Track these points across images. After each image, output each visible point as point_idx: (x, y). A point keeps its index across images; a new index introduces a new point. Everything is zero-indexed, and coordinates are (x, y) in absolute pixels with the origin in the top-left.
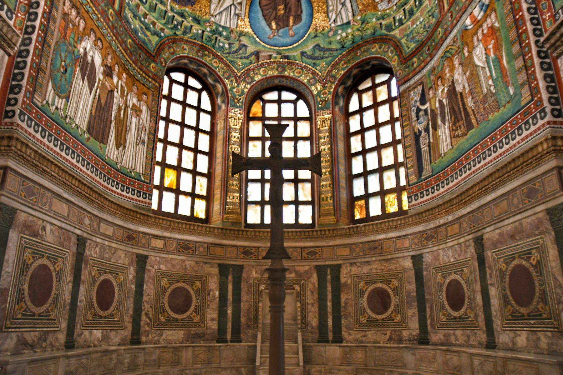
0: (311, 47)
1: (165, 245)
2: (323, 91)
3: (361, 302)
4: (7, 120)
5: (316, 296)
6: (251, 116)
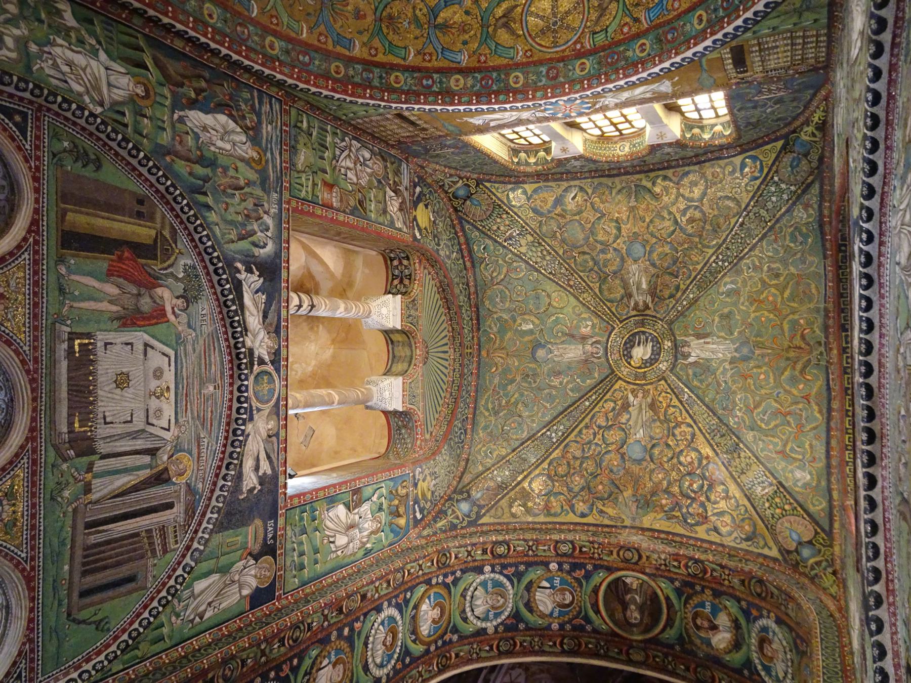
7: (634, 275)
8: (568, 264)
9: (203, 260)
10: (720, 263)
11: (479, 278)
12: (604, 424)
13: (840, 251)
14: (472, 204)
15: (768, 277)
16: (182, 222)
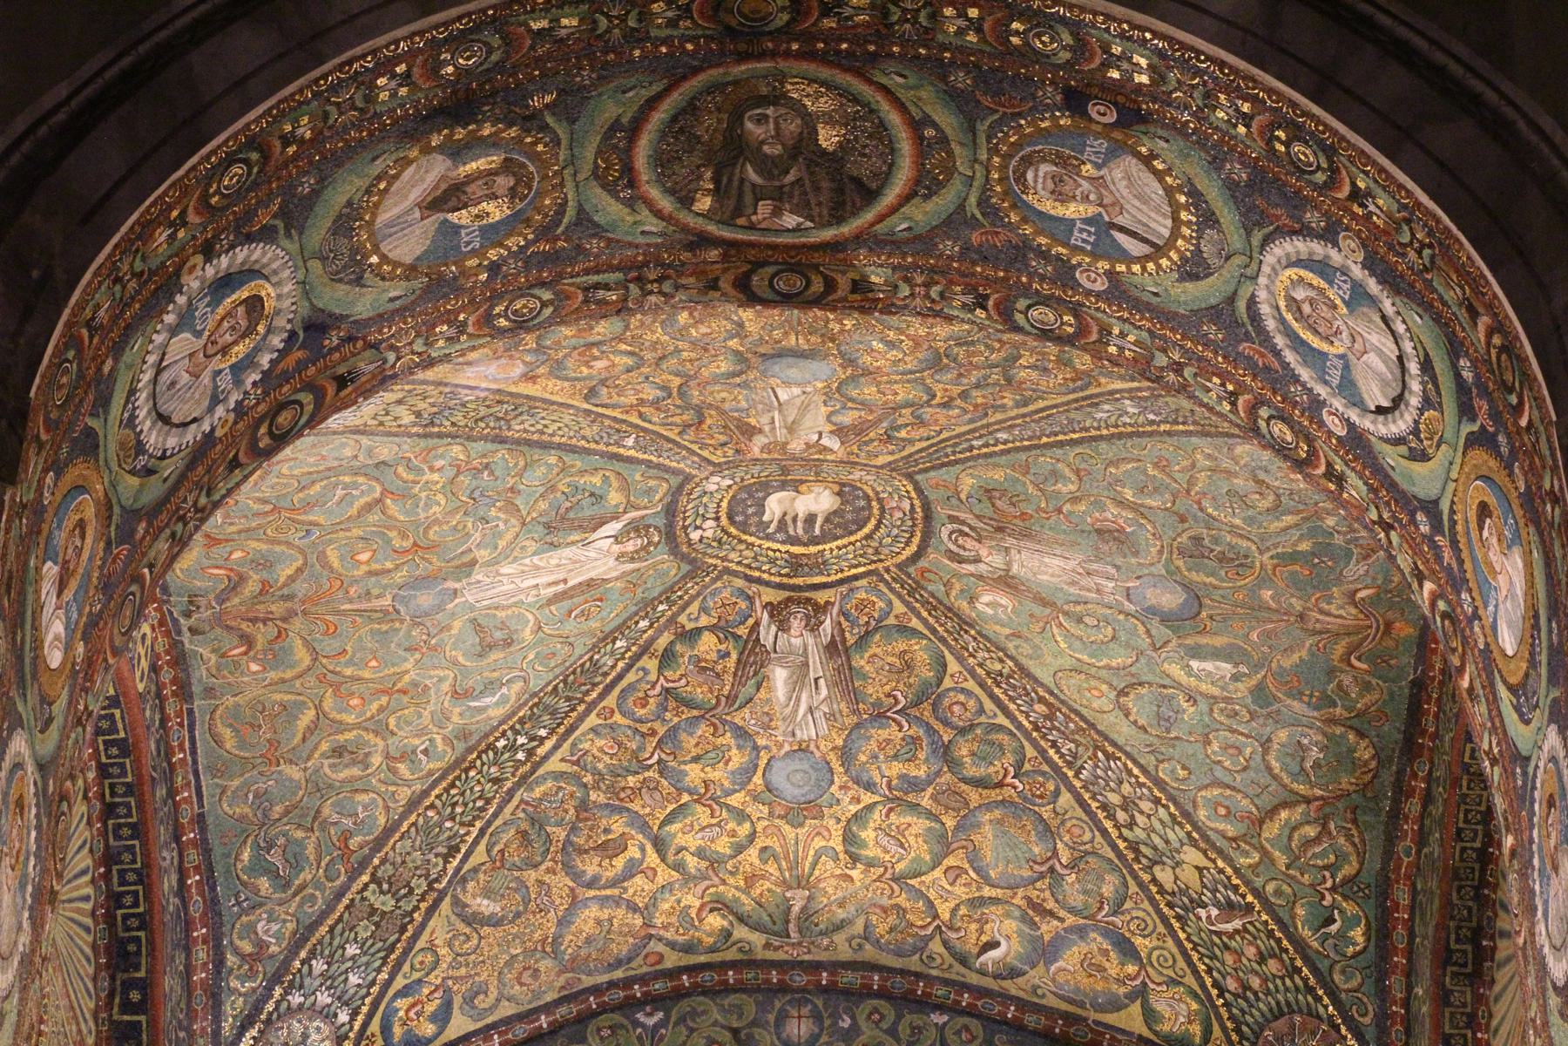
7: (811, 710)
8: (1049, 761)
10: (521, 740)
12: (927, 413)
15: (367, 743)
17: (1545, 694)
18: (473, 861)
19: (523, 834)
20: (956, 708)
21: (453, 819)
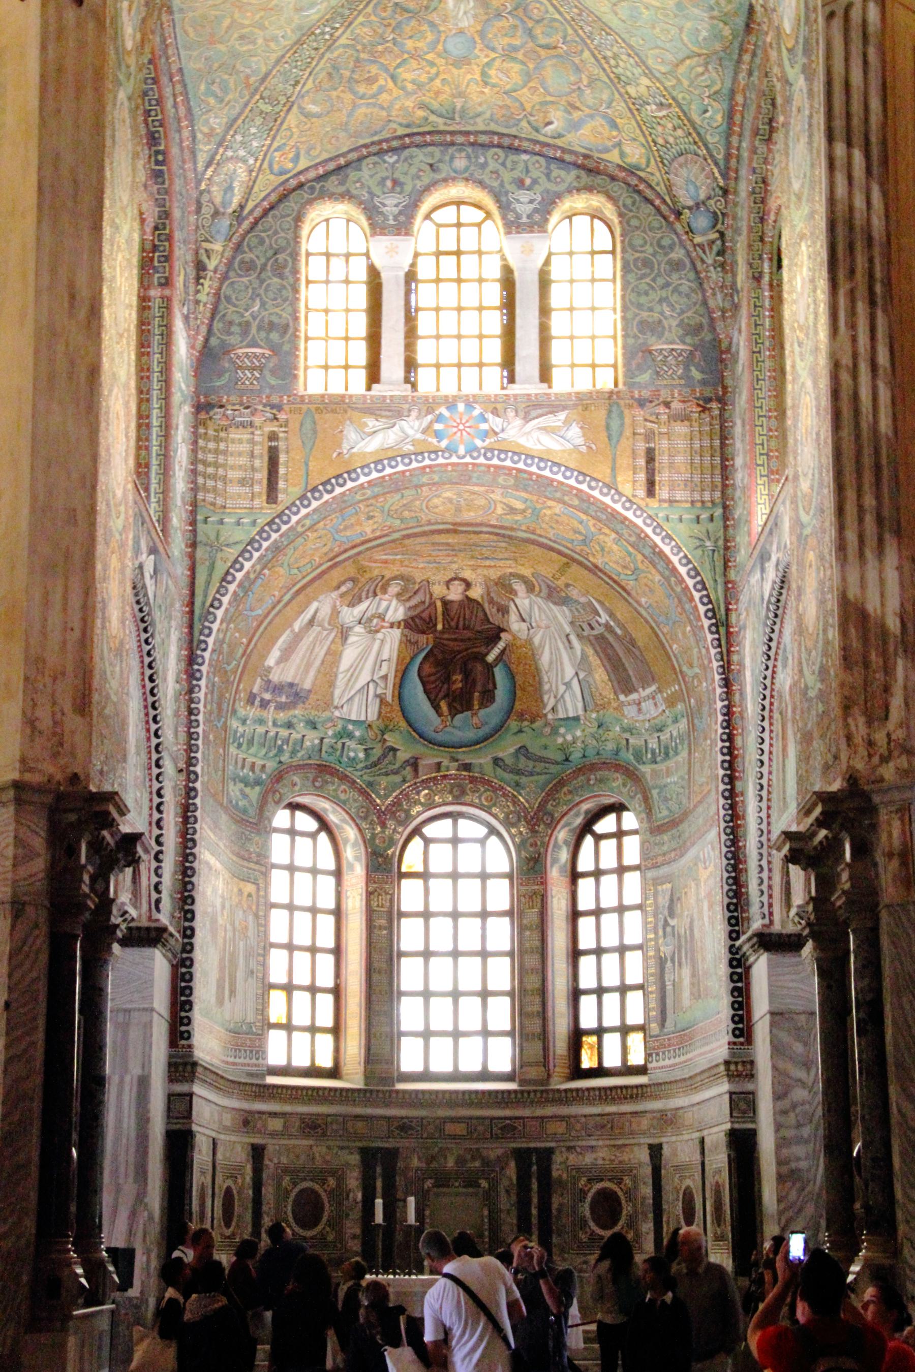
0: (512, 750)
1: (285, 1126)
2: (531, 840)
3: (581, 1209)
4: (183, 1042)
5: (514, 1198)
6: (404, 869)
7: (465, 13)
8: (578, 35)
9: (776, 654)
10: (327, 29)
11: (729, 73)
13: (164, 153)
14: (697, 188)
16: (772, 690)
17: (801, 60)
18: (306, 88)
19: (330, 74)
20: (535, 11)
21: (296, 67)
